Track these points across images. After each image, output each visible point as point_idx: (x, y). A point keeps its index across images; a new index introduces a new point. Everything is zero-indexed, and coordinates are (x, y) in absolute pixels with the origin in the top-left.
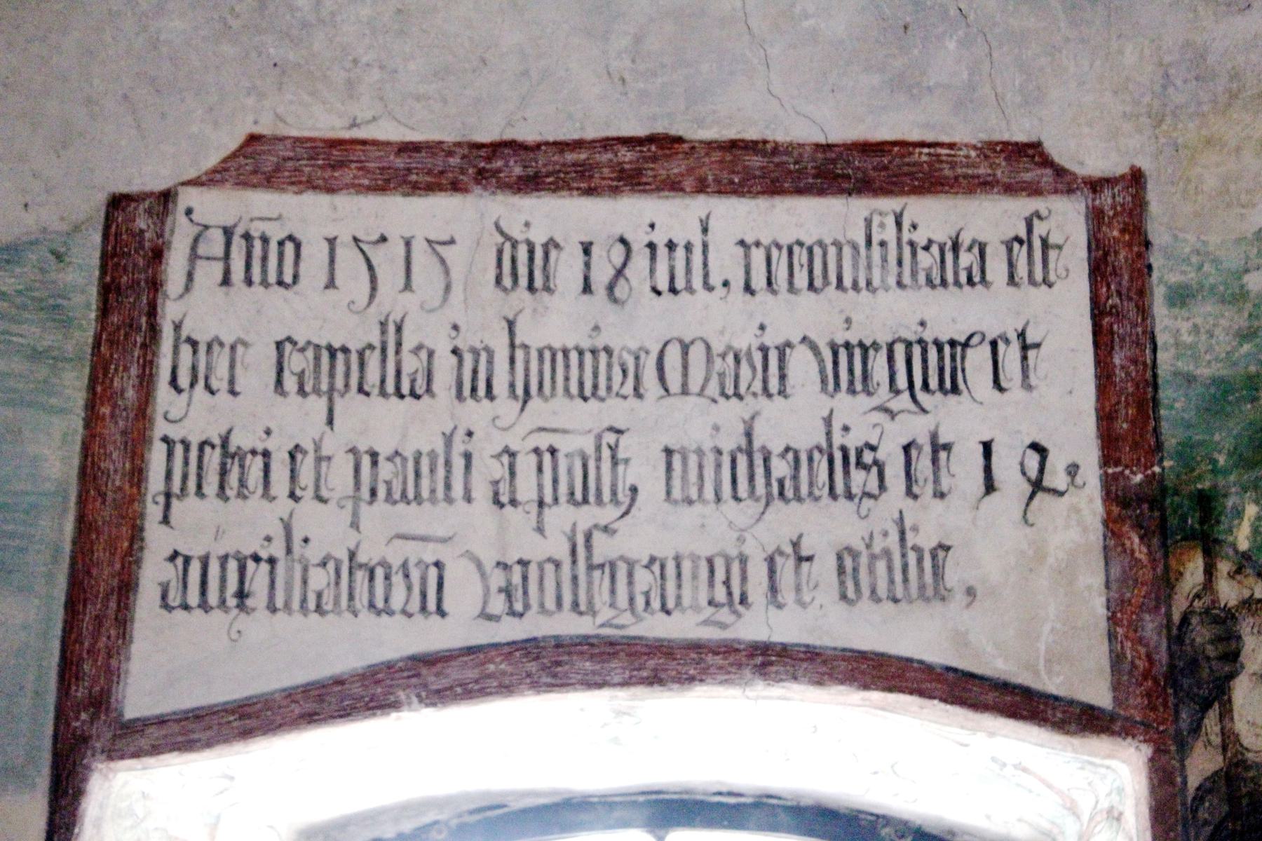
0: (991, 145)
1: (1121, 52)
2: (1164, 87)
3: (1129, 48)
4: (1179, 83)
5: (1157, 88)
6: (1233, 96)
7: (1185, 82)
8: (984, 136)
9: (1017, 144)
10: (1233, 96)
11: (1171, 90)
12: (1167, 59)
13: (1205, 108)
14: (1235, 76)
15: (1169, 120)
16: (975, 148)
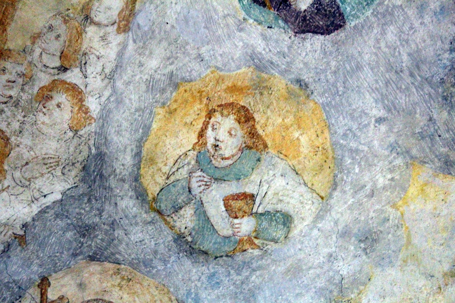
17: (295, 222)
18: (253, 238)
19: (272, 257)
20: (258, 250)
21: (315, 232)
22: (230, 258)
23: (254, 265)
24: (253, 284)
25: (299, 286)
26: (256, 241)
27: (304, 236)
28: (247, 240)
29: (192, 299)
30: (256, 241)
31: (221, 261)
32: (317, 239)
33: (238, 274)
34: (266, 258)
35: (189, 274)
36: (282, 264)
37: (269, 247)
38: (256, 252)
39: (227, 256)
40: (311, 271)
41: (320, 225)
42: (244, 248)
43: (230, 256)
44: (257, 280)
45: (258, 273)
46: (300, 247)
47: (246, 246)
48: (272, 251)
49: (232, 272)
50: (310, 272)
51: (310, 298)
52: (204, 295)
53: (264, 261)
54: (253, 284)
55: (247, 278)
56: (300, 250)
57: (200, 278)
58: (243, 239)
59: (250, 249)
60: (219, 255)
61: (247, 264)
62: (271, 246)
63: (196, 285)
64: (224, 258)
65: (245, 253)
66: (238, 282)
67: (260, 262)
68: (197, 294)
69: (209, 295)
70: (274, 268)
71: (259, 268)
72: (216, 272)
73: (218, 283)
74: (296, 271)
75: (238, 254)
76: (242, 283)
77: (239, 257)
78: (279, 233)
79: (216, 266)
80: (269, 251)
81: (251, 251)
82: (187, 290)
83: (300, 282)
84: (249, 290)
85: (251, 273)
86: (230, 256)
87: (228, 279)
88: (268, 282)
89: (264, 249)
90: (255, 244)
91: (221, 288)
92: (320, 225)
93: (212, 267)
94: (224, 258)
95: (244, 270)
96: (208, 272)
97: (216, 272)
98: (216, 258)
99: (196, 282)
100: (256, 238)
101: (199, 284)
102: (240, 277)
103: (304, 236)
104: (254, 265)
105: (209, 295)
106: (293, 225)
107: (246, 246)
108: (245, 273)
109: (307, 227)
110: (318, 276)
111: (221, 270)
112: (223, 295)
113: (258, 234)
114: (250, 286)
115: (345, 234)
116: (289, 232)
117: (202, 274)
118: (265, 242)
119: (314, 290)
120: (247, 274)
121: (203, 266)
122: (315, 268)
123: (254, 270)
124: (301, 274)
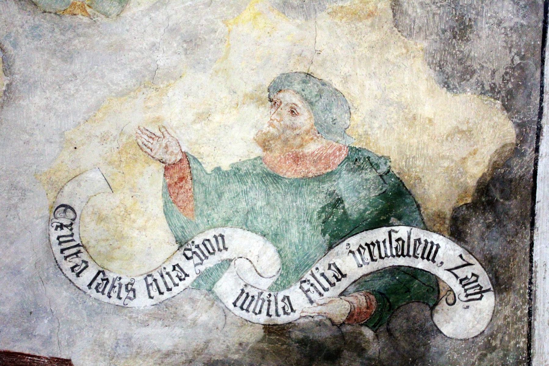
0: (53, 358)
1: (104, 333)
2: (116, 347)
3: (106, 332)
4: (121, 346)
5: (114, 347)
6: (138, 354)
7: (123, 346)
8: (51, 355)
9: (62, 359)
10: (138, 354)
11: (118, 348)
12: (119, 337)
13: (128, 356)
14: (139, 348)
15: (115, 359)
16: (47, 359)
17: (131, 5)
18: (86, 5)
19: (100, 29)
20: (87, 18)
21: (147, 19)
22: (58, 17)
23: (80, 31)
24: (74, 47)
25: (116, 62)
26: (89, 10)
27: (135, 20)
28: (80, 5)
29: (10, 42)
30: (89, 10)
31: (48, 16)
32: (146, 26)
33: (61, 34)
34: (93, 28)
35: (13, 18)
36: (107, 38)
37: (99, 19)
38: (86, 20)
39: (56, 14)
40: (132, 53)
41: (153, 15)
42: (75, 12)
43: (59, 15)
44: (78, 45)
45: (82, 39)
46: (128, 28)
47: (77, 11)
48: (101, 24)
49: (57, 30)
50: (130, 53)
51: (123, 76)
52: (23, 42)
53: (90, 29)
54: (74, 47)
55: (70, 40)
56: (127, 30)
57: (23, 25)
58: (76, 3)
59: (80, 14)
60: (48, 11)
61: (73, 28)
62: (101, 19)
63: (17, 31)
64: (52, 15)
65: (75, 16)
66: (59, 41)
67: (86, 30)
68: (15, 39)
69: (28, 43)
70: (98, 39)
71: (85, 35)
72: (41, 25)
73: (40, 36)
74: (119, 48)
75: (67, 16)
76: (64, 43)
77: (68, 19)
78: (113, 10)
79: (43, 20)
80: (98, 23)
81: (82, 17)
82: (6, 32)
83: (118, 59)
84: (68, 51)
85: (74, 37)
86: (59, 15)
87: (50, 35)
88: (89, 50)
89: (94, 19)
90: (87, 12)
91: (41, 41)
92: (153, 15)
93: (38, 19)
94: (52, 15)
95: (69, 32)
96: (32, 21)
97: (41, 25)
98: (45, 12)
99: (18, 28)
100: (89, 6)
101: (21, 31)
102: (63, 37)
103: (135, 20)
104: (80, 31)
105: (28, 43)
106: (128, 6)
107: (77, 11)
108: (70, 34)
109: (140, 13)
110: (137, 59)
111: (47, 25)
112: (42, 48)
113: (91, 4)
114: (71, 48)
115: (173, 31)
116: (122, 11)
117: (27, 22)
118: (97, 13)
119: (128, 70)
120: (71, 36)
121: (29, 15)
122: (136, 51)
123: (79, 35)
124: (121, 52)
